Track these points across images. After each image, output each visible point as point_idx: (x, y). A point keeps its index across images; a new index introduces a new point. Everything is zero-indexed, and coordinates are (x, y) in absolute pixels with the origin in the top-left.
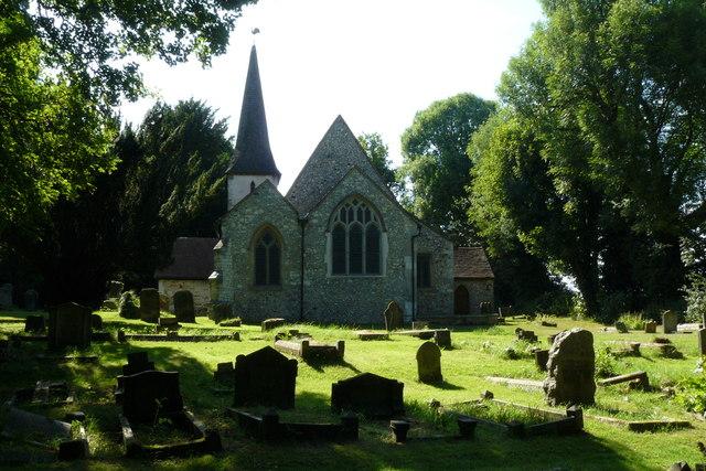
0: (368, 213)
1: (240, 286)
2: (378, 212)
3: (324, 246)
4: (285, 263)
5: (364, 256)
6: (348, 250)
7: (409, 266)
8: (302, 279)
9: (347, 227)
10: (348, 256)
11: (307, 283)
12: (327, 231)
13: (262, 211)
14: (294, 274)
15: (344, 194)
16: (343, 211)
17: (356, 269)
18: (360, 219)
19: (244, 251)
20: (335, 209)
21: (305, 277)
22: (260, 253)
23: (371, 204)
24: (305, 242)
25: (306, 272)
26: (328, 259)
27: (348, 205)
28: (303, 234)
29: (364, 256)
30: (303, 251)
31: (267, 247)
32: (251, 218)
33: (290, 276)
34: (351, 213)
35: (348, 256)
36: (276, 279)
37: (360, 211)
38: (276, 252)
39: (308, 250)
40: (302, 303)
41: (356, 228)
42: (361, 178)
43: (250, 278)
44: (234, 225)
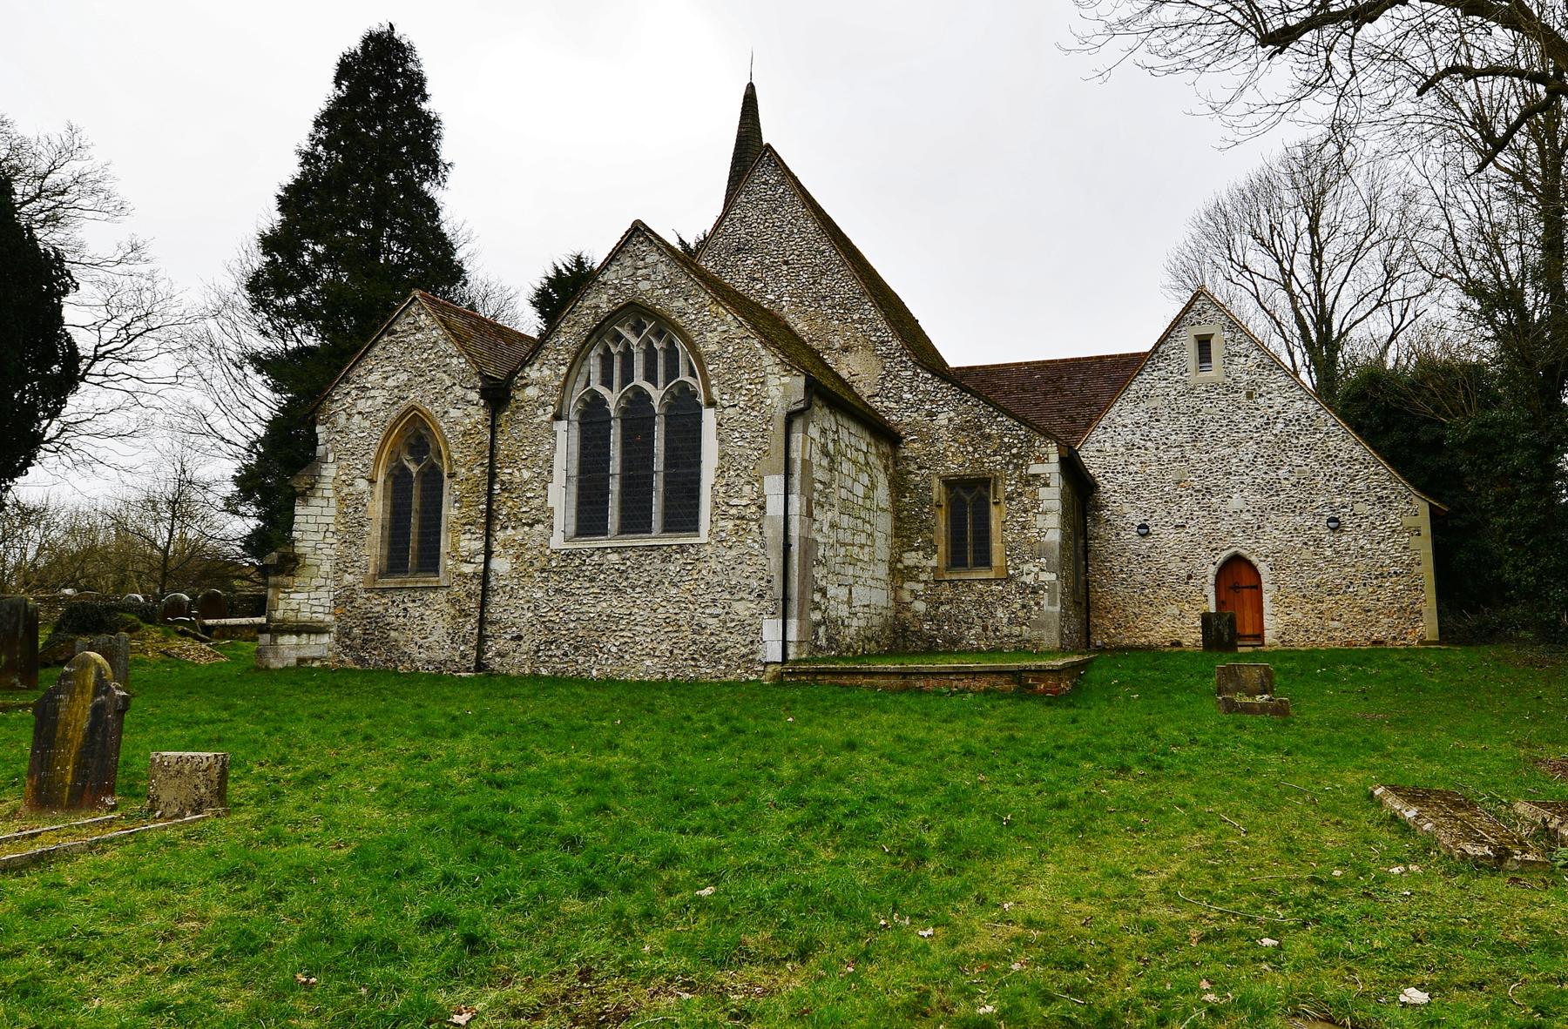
0: (672, 354)
1: (348, 579)
2: (692, 347)
3: (549, 461)
4: (450, 512)
5: (658, 483)
6: (615, 466)
7: (775, 507)
8: (488, 554)
9: (612, 399)
10: (615, 486)
11: (501, 565)
12: (557, 417)
13: (404, 377)
14: (471, 543)
15: (605, 308)
16: (607, 359)
17: (636, 521)
18: (651, 376)
19: (362, 485)
20: (580, 357)
21: (497, 548)
22: (399, 482)
23: (679, 330)
24: (503, 450)
25: (500, 535)
26: (560, 498)
27: (618, 338)
28: (493, 429)
29: (658, 483)
30: (492, 477)
31: (413, 468)
32: (381, 397)
33: (460, 544)
34: (627, 357)
35: (615, 486)
36: (430, 560)
37: (650, 355)
38: (433, 481)
39: (504, 474)
40: (482, 622)
41: (641, 397)
42: (652, 258)
43: (372, 550)
44: (342, 419)
